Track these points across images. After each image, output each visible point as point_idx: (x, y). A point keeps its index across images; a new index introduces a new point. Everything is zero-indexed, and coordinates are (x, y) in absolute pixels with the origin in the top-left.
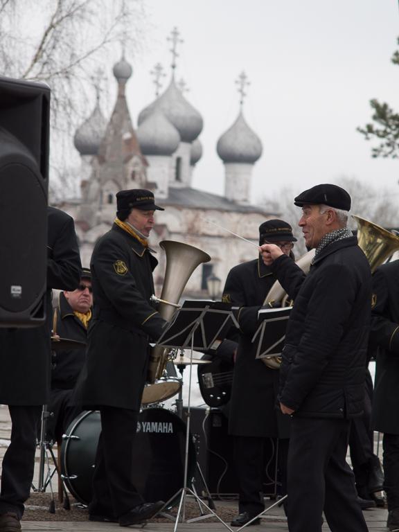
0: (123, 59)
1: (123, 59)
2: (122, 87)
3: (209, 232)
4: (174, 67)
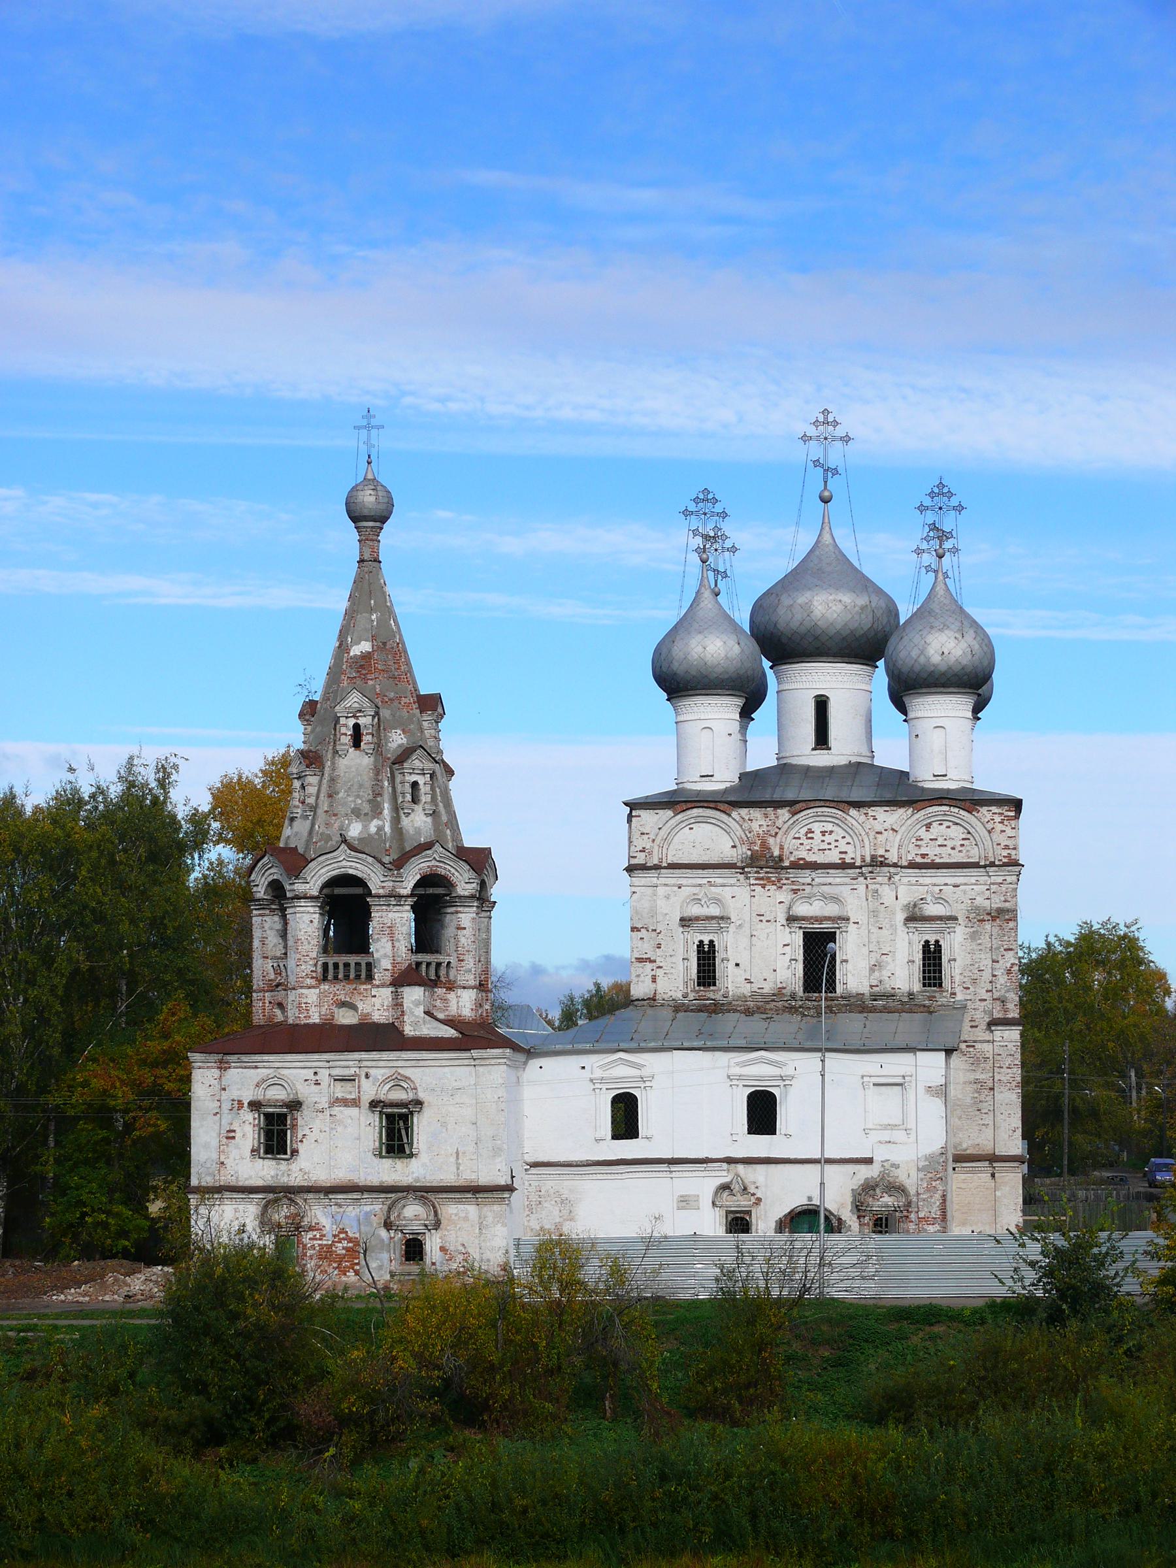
3: (811, 858)
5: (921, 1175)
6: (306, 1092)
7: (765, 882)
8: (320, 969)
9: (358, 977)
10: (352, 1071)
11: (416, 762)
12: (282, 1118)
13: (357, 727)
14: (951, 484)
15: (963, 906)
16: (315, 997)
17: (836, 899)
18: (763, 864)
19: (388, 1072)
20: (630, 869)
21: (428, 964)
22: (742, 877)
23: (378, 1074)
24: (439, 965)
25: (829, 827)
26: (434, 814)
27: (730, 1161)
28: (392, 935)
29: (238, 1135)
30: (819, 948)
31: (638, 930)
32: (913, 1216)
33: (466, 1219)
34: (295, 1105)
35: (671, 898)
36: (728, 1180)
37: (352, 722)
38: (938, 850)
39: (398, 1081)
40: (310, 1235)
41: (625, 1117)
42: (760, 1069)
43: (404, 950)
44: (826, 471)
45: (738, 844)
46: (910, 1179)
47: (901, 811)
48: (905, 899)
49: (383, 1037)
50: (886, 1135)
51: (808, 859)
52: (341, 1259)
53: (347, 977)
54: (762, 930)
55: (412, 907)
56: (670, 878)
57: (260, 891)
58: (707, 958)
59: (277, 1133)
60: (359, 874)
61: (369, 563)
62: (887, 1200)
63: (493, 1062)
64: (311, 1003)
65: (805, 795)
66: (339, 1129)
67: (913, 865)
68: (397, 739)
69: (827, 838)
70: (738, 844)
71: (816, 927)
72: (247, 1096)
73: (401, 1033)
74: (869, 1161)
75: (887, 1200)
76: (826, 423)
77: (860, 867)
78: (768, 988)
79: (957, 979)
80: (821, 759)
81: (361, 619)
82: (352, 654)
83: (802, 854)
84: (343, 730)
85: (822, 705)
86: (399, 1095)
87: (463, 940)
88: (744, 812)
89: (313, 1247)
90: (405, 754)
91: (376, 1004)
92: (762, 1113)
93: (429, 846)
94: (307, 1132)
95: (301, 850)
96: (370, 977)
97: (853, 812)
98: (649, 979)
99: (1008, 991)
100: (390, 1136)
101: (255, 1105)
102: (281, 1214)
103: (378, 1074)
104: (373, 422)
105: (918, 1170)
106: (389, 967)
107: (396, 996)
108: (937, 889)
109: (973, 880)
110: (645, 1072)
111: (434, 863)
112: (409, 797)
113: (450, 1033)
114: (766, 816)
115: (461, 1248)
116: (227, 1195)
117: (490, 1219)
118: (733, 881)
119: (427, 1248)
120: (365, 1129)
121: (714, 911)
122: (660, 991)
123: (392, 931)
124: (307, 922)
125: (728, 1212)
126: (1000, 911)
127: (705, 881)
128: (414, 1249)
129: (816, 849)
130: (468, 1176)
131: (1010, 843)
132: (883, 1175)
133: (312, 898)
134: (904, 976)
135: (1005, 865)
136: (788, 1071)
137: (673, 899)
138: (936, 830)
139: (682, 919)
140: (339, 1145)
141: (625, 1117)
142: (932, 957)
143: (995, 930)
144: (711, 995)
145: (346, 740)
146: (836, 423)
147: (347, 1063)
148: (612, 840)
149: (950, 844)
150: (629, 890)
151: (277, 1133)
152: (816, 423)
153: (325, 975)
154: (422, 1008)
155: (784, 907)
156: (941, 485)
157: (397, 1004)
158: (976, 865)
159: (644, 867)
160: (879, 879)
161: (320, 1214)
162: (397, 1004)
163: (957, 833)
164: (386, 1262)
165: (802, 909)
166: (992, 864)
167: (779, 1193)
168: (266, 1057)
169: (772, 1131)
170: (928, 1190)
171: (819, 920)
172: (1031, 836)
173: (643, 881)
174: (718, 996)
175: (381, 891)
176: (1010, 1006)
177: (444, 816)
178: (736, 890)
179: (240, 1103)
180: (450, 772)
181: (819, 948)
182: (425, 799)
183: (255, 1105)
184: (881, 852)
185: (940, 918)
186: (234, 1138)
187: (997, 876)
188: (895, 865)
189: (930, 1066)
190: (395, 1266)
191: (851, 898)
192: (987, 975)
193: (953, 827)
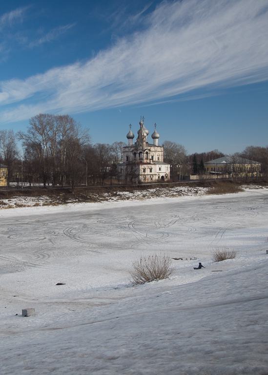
42: (160, 166)
49: (150, 164)
91: (148, 161)
92: (160, 169)
120: (149, 170)
128: (152, 179)
134: (157, 160)
151: (144, 171)
167: (161, 175)
181: (152, 157)
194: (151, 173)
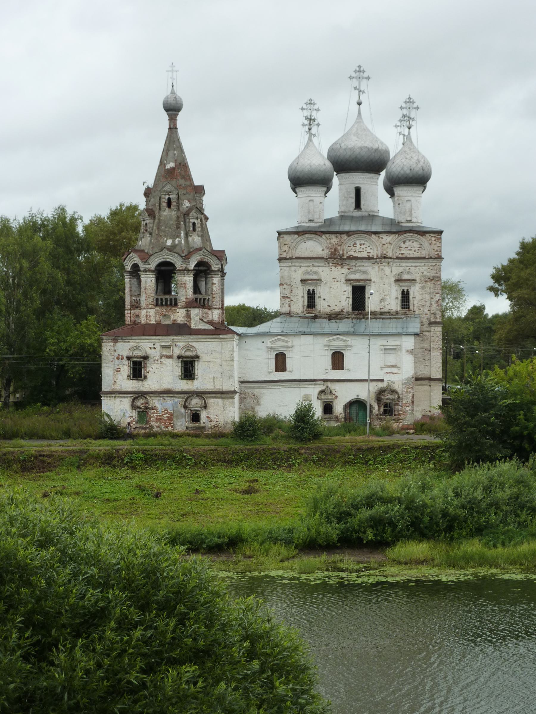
0: (173, 92)
1: (173, 92)
2: (173, 119)
3: (355, 255)
4: (359, 104)
5: (404, 386)
6: (151, 353)
7: (336, 265)
8: (155, 301)
9: (171, 304)
10: (169, 344)
11: (193, 214)
12: (140, 363)
13: (169, 199)
14: (414, 98)
15: (418, 275)
16: (153, 313)
17: (365, 272)
18: (336, 258)
19: (185, 344)
20: (280, 260)
21: (200, 299)
22: (326, 263)
23: (181, 345)
24: (204, 299)
25: (363, 242)
26: (202, 236)
27: (325, 381)
28: (185, 287)
29: (122, 370)
30: (359, 293)
31: (283, 285)
32: (400, 403)
33: (218, 404)
34: (146, 358)
35: (297, 273)
36: (323, 388)
37: (167, 197)
38: (408, 252)
39: (188, 348)
40: (152, 411)
41: (281, 362)
43: (191, 293)
44: (360, 91)
45: (325, 248)
46: (398, 387)
47: (393, 235)
48: (394, 273)
49: (183, 329)
50: (389, 370)
51: (354, 255)
52: (165, 421)
53: (171, 304)
54: (335, 285)
55: (194, 275)
56: (297, 263)
57: (128, 268)
58: (311, 297)
59: (138, 370)
60: (172, 261)
61: (173, 129)
62: (390, 397)
63: (229, 340)
64: (149, 315)
65: (353, 228)
66: (164, 367)
67: (398, 258)
68: (186, 204)
69: (362, 247)
70: (325, 248)
71: (357, 284)
72: (125, 354)
73: (190, 328)
74: (382, 381)
75: (390, 397)
76: (360, 71)
77: (376, 259)
78: (337, 309)
79: (416, 305)
80: (357, 213)
81: (170, 153)
82: (166, 168)
83: (351, 253)
84: (164, 200)
85: (358, 191)
86: (189, 354)
87: (215, 289)
88: (327, 235)
89: (153, 416)
90: (190, 210)
91: (179, 316)
92: (338, 360)
93: (199, 249)
94: (150, 369)
95: (146, 251)
96: (176, 305)
97: (373, 236)
98: (287, 305)
99: (437, 310)
100: (186, 370)
101: (129, 358)
102: (140, 403)
103: (181, 345)
104: (175, 69)
105: (403, 384)
106: (184, 300)
107: (188, 311)
108: (408, 268)
109: (423, 264)
110: (290, 344)
111: (202, 256)
112: (191, 229)
113: (210, 327)
114: (337, 237)
115: (215, 417)
116: (118, 395)
117: (228, 405)
118: (322, 265)
119: (201, 416)
121: (315, 277)
122: (292, 310)
123: (184, 285)
124: (149, 281)
125: (324, 402)
126: (434, 277)
127: (311, 264)
128: (196, 417)
129: (357, 251)
130: (218, 387)
131: (438, 249)
132: (388, 387)
133: (152, 271)
134: (394, 304)
135: (436, 258)
136: (349, 343)
137: (297, 272)
138: (408, 244)
139: (301, 281)
140: (163, 375)
141: (281, 362)
142: (405, 297)
143: (432, 285)
144: (314, 312)
145: (164, 205)
146: (364, 71)
147: (168, 340)
148: (274, 249)
149: (413, 249)
150: (279, 268)
151: (138, 370)
152: (355, 71)
153: (157, 303)
154: (198, 318)
155: (343, 276)
156: (410, 98)
157: (188, 315)
158: (424, 258)
159: (285, 259)
160: (384, 264)
161: (155, 402)
162: (188, 315)
163: (416, 245)
164: (184, 422)
165: (352, 277)
166: (431, 258)
168: (133, 338)
169: (342, 368)
170: (407, 392)
171: (358, 280)
172: (448, 247)
173: (285, 265)
174: (316, 313)
175: (181, 268)
176: (438, 316)
177: (205, 236)
178: (324, 269)
179: (122, 357)
180: (207, 219)
181: (359, 293)
182: (198, 229)
183: (129, 358)
184: (385, 252)
185: (409, 280)
186: (120, 371)
187: (432, 263)
188: (390, 258)
189: (408, 343)
190: (187, 424)
191: (373, 272)
192: (428, 304)
193: (415, 242)
194: (185, 385)
